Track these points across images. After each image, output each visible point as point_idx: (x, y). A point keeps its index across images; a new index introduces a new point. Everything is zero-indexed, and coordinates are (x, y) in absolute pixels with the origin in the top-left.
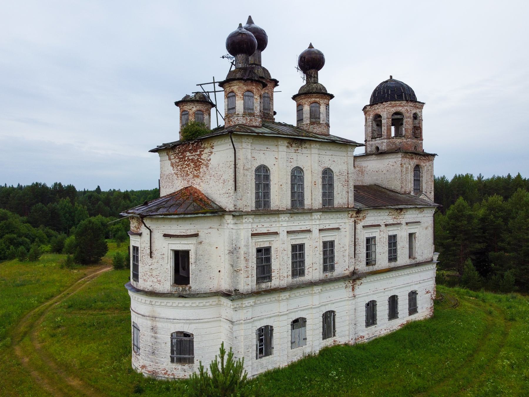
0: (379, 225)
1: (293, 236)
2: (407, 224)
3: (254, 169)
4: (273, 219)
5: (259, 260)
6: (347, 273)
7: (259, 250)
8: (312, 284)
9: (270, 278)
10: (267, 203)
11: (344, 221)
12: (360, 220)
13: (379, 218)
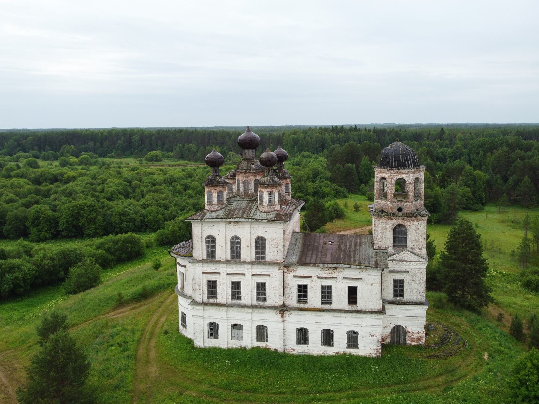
0: (310, 277)
1: (231, 276)
2: (344, 278)
3: (204, 237)
4: (217, 265)
5: (208, 287)
6: (277, 305)
7: (209, 282)
8: (244, 306)
9: (216, 297)
10: (214, 257)
11: (274, 271)
12: (291, 271)
13: (311, 272)
